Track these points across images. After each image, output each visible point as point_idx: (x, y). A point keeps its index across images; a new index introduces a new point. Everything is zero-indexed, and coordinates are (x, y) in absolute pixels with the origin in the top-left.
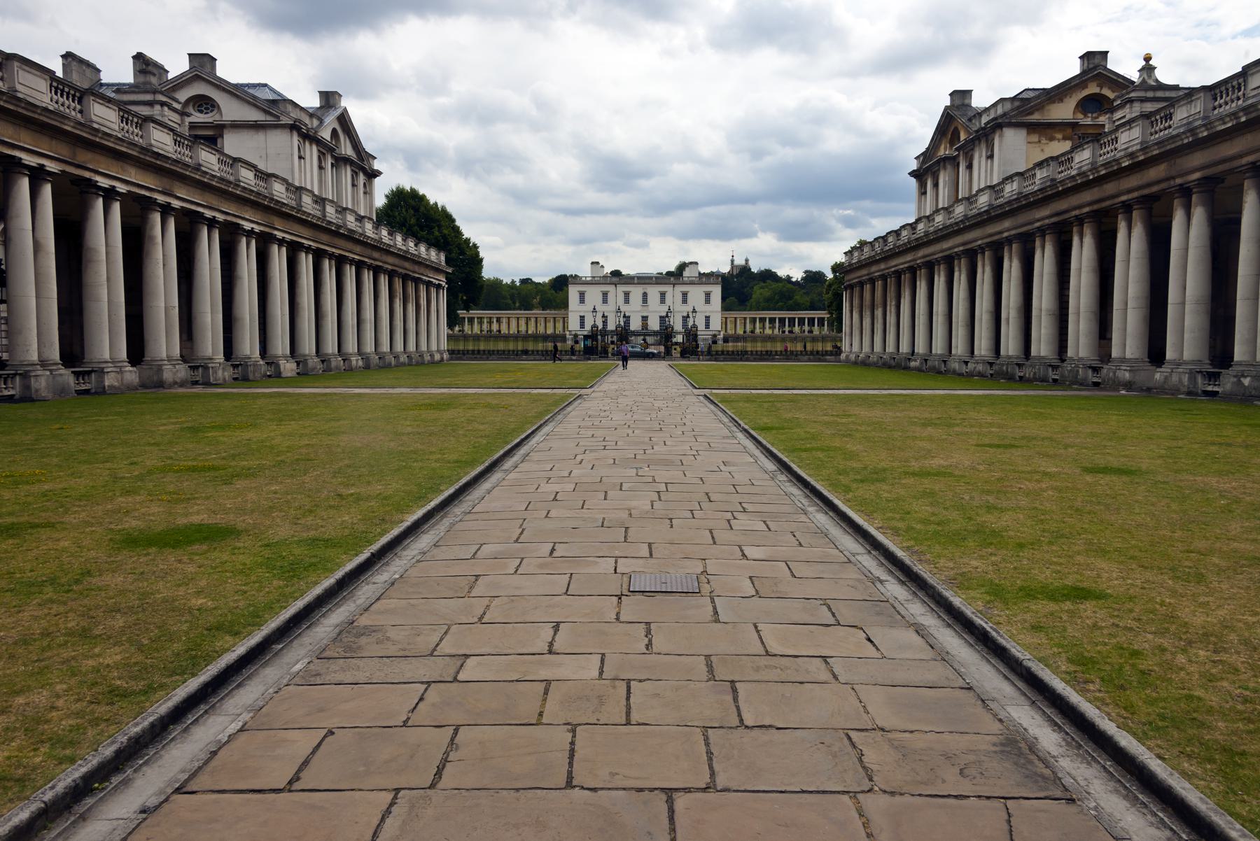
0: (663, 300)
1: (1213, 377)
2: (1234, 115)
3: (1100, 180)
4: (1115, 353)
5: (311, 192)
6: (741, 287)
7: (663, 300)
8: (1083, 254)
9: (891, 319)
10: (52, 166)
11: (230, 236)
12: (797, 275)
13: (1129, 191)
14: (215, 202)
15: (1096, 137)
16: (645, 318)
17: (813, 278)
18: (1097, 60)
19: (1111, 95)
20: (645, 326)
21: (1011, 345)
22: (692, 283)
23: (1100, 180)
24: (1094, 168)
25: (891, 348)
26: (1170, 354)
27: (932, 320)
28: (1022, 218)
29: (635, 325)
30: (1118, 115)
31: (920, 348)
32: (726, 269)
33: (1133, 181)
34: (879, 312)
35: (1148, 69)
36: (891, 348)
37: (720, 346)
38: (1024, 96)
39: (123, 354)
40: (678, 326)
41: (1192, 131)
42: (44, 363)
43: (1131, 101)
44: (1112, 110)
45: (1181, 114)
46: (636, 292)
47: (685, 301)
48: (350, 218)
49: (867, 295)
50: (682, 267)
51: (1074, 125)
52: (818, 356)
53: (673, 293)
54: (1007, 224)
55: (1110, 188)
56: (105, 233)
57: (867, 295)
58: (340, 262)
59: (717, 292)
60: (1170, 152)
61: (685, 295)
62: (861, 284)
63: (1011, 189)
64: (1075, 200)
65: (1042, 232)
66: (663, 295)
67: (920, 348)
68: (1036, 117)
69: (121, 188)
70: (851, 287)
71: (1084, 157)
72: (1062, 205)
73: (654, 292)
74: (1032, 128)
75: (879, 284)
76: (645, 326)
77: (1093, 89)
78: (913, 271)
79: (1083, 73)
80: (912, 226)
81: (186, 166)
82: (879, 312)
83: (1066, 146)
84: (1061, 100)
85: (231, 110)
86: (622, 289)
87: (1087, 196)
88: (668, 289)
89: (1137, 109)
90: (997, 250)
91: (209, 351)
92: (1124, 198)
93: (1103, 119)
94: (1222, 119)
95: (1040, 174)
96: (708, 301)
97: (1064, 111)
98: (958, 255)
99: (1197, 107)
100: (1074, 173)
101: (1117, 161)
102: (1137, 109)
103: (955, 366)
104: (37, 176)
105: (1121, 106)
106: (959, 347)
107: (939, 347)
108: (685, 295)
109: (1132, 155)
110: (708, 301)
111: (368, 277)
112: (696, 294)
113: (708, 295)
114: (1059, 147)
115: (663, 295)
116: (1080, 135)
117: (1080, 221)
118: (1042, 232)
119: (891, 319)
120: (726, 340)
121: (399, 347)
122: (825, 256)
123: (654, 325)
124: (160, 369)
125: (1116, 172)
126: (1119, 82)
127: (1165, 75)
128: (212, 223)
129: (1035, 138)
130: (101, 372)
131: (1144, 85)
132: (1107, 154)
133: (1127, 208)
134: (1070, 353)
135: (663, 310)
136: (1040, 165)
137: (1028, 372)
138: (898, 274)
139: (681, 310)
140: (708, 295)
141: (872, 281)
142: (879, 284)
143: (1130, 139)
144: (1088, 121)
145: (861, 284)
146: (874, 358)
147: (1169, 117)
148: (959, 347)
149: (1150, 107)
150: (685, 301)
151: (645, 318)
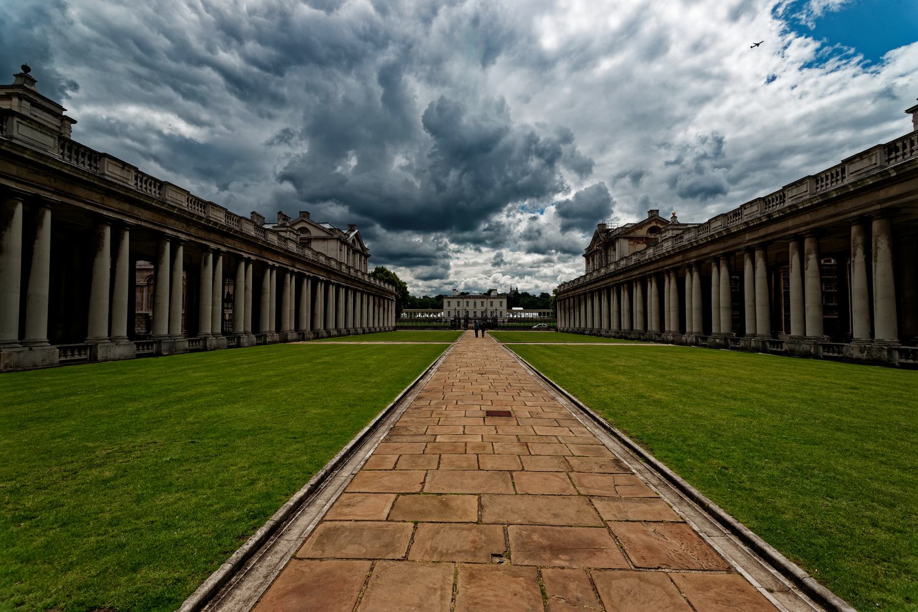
0: (482, 305)
1: (705, 339)
2: (706, 238)
3: (657, 261)
4: (666, 329)
5: (336, 260)
6: (515, 298)
7: (482, 305)
8: (652, 290)
9: (577, 314)
10: (253, 258)
11: (315, 282)
12: (538, 295)
13: (669, 265)
14: (310, 269)
16: (475, 312)
17: (545, 296)
20: (475, 316)
21: (625, 325)
22: (494, 298)
23: (657, 261)
25: (577, 326)
26: (688, 330)
27: (593, 313)
28: (627, 275)
29: (471, 315)
31: (589, 326)
32: (508, 292)
33: (670, 261)
34: (572, 311)
36: (577, 326)
37: (506, 324)
39: (274, 329)
40: (489, 316)
41: (691, 244)
42: (245, 333)
44: (661, 233)
45: (686, 237)
46: (471, 301)
47: (492, 305)
48: (359, 274)
49: (567, 304)
50: (490, 291)
52: (549, 328)
53: (487, 302)
54: (622, 277)
55: (661, 264)
56: (270, 282)
57: (567, 304)
58: (355, 291)
59: (505, 301)
60: (684, 251)
61: (492, 303)
62: (564, 299)
63: (623, 263)
65: (636, 280)
66: (482, 303)
67: (589, 326)
69: (277, 265)
70: (560, 301)
72: (643, 270)
73: (479, 301)
75: (572, 300)
76: (475, 316)
78: (585, 294)
80: (584, 277)
81: (300, 256)
82: (572, 311)
85: (314, 232)
86: (465, 300)
87: (652, 267)
88: (485, 300)
89: (669, 234)
90: (618, 287)
91: (305, 328)
95: (634, 258)
96: (501, 305)
98: (603, 289)
99: (692, 234)
102: (669, 234)
103: (603, 333)
104: (248, 261)
106: (605, 325)
107: (596, 326)
108: (492, 303)
110: (501, 305)
111: (365, 297)
112: (496, 302)
113: (501, 303)
114: (641, 247)
115: (482, 303)
116: (651, 243)
117: (650, 276)
118: (636, 280)
119: (577, 314)
120: (509, 321)
121: (376, 325)
122: (549, 287)
123: (479, 315)
124: (287, 335)
126: (665, 222)
128: (308, 277)
130: (266, 336)
133: (668, 272)
134: (649, 328)
135: (483, 309)
136: (633, 254)
137: (632, 336)
138: (579, 295)
139: (490, 309)
140: (501, 303)
141: (569, 298)
142: (572, 300)
145: (564, 299)
146: (570, 330)
147: (682, 238)
148: (605, 325)
149: (676, 232)
150: (492, 305)
151: (475, 312)
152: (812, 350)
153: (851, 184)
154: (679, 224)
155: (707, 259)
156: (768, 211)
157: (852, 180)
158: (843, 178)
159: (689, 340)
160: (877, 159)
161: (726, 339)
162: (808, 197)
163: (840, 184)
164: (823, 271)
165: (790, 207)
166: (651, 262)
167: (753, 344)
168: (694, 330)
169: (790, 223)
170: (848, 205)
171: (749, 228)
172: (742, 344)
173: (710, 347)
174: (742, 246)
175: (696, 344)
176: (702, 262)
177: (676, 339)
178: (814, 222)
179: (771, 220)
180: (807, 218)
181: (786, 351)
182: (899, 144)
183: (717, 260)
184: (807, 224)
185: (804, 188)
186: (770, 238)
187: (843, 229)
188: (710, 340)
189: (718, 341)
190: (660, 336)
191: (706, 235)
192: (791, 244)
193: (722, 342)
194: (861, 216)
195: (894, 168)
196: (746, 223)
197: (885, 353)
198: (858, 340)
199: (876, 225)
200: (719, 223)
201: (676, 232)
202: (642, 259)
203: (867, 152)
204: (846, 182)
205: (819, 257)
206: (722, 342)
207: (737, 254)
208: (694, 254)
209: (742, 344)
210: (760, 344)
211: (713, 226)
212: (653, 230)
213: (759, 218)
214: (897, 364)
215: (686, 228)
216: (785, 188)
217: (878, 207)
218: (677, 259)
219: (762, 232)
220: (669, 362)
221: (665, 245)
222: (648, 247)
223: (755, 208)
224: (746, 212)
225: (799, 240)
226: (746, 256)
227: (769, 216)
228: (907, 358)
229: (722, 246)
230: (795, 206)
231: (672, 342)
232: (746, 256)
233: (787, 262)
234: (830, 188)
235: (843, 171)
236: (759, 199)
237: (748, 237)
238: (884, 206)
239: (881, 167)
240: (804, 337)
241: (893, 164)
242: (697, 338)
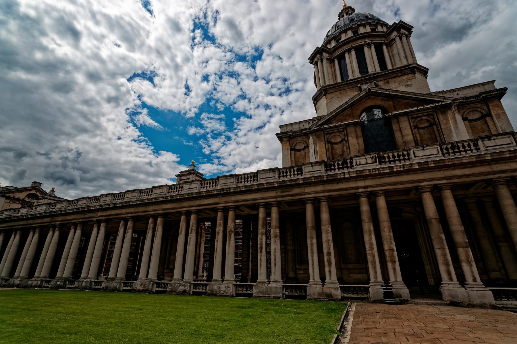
2: (73, 209)
15: (30, 206)
18: (37, 185)
19: (39, 195)
24: (27, 215)
30: (40, 201)
33: (39, 221)
35: (53, 191)
38: (8, 188)
41: (61, 211)
43: (45, 199)
45: (59, 206)
51: (24, 201)
55: (30, 222)
60: (53, 215)
64: (16, 223)
68: (11, 195)
71: (24, 211)
74: (8, 198)
77: (34, 192)
79: (32, 187)
83: (20, 206)
84: (22, 192)
89: (46, 201)
92: (34, 225)
93: (34, 201)
94: (70, 210)
95: (6, 213)
97: (22, 196)
99: (64, 205)
100: (19, 215)
101: (36, 214)
102: (46, 201)
105: (42, 199)
109: (41, 214)
116: (24, 204)
125: (34, 217)
126: (43, 193)
127: (57, 194)
129: (8, 201)
131: (50, 195)
132: (33, 212)
136: (7, 210)
143: (41, 209)
144: (29, 200)
149: (50, 201)
152: (118, 287)
153: (155, 198)
154: (55, 197)
155: (69, 223)
156: (115, 202)
157: (154, 197)
158: (151, 195)
159: (35, 283)
160: (165, 190)
161: (65, 282)
162: (135, 199)
163: (150, 197)
164: (133, 239)
165: (126, 202)
166: (22, 219)
167: (84, 284)
168: (41, 276)
169: (124, 211)
170: (151, 208)
171: (102, 209)
172: (76, 284)
173: (51, 288)
174: (95, 219)
175: (40, 287)
176: (65, 224)
177: (24, 283)
178: (135, 213)
179: (115, 207)
180: (132, 210)
181: (103, 288)
182: (173, 187)
183: (76, 225)
184: (132, 213)
185: (134, 194)
186: (112, 217)
187: (147, 218)
188: (53, 282)
189: (58, 283)
190: (6, 280)
191: (73, 207)
192: (121, 222)
193: (62, 284)
194: (154, 214)
195: (170, 196)
196: (101, 206)
197: (151, 285)
198: (141, 279)
199: (159, 220)
200: (84, 202)
201: (50, 201)
202: (13, 215)
203: (162, 186)
204: (152, 197)
205: (133, 232)
206: (62, 284)
207: (89, 223)
208: (60, 218)
209: (76, 284)
210: (88, 284)
211: (80, 202)
212: (29, 196)
213: (109, 205)
214: (154, 291)
215: (60, 201)
216: (126, 192)
217: (161, 212)
218: (46, 220)
219: (108, 213)
220: (11, 305)
221: (39, 208)
222: (23, 207)
223: (108, 198)
224: (102, 199)
225: (126, 220)
226: (95, 225)
227: (115, 204)
228: (159, 288)
229: (82, 217)
230: (129, 202)
231: (18, 286)
232: (95, 225)
233: (116, 233)
234: (145, 198)
235: (152, 192)
236: (112, 194)
237: (99, 214)
238: (164, 212)
239: (166, 194)
240: (115, 278)
241: (170, 194)
242: (42, 281)
